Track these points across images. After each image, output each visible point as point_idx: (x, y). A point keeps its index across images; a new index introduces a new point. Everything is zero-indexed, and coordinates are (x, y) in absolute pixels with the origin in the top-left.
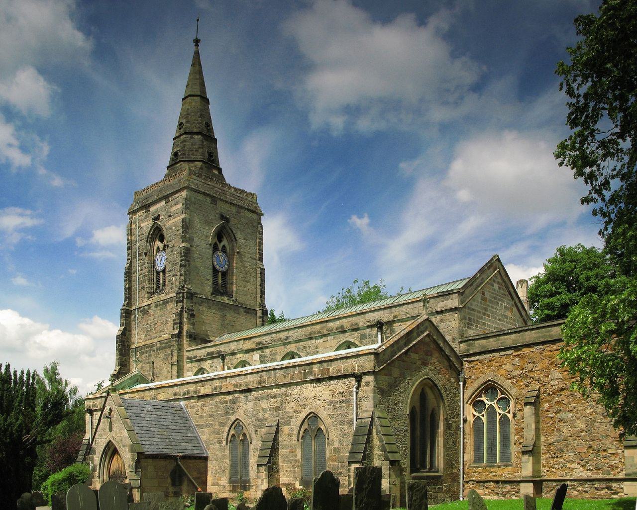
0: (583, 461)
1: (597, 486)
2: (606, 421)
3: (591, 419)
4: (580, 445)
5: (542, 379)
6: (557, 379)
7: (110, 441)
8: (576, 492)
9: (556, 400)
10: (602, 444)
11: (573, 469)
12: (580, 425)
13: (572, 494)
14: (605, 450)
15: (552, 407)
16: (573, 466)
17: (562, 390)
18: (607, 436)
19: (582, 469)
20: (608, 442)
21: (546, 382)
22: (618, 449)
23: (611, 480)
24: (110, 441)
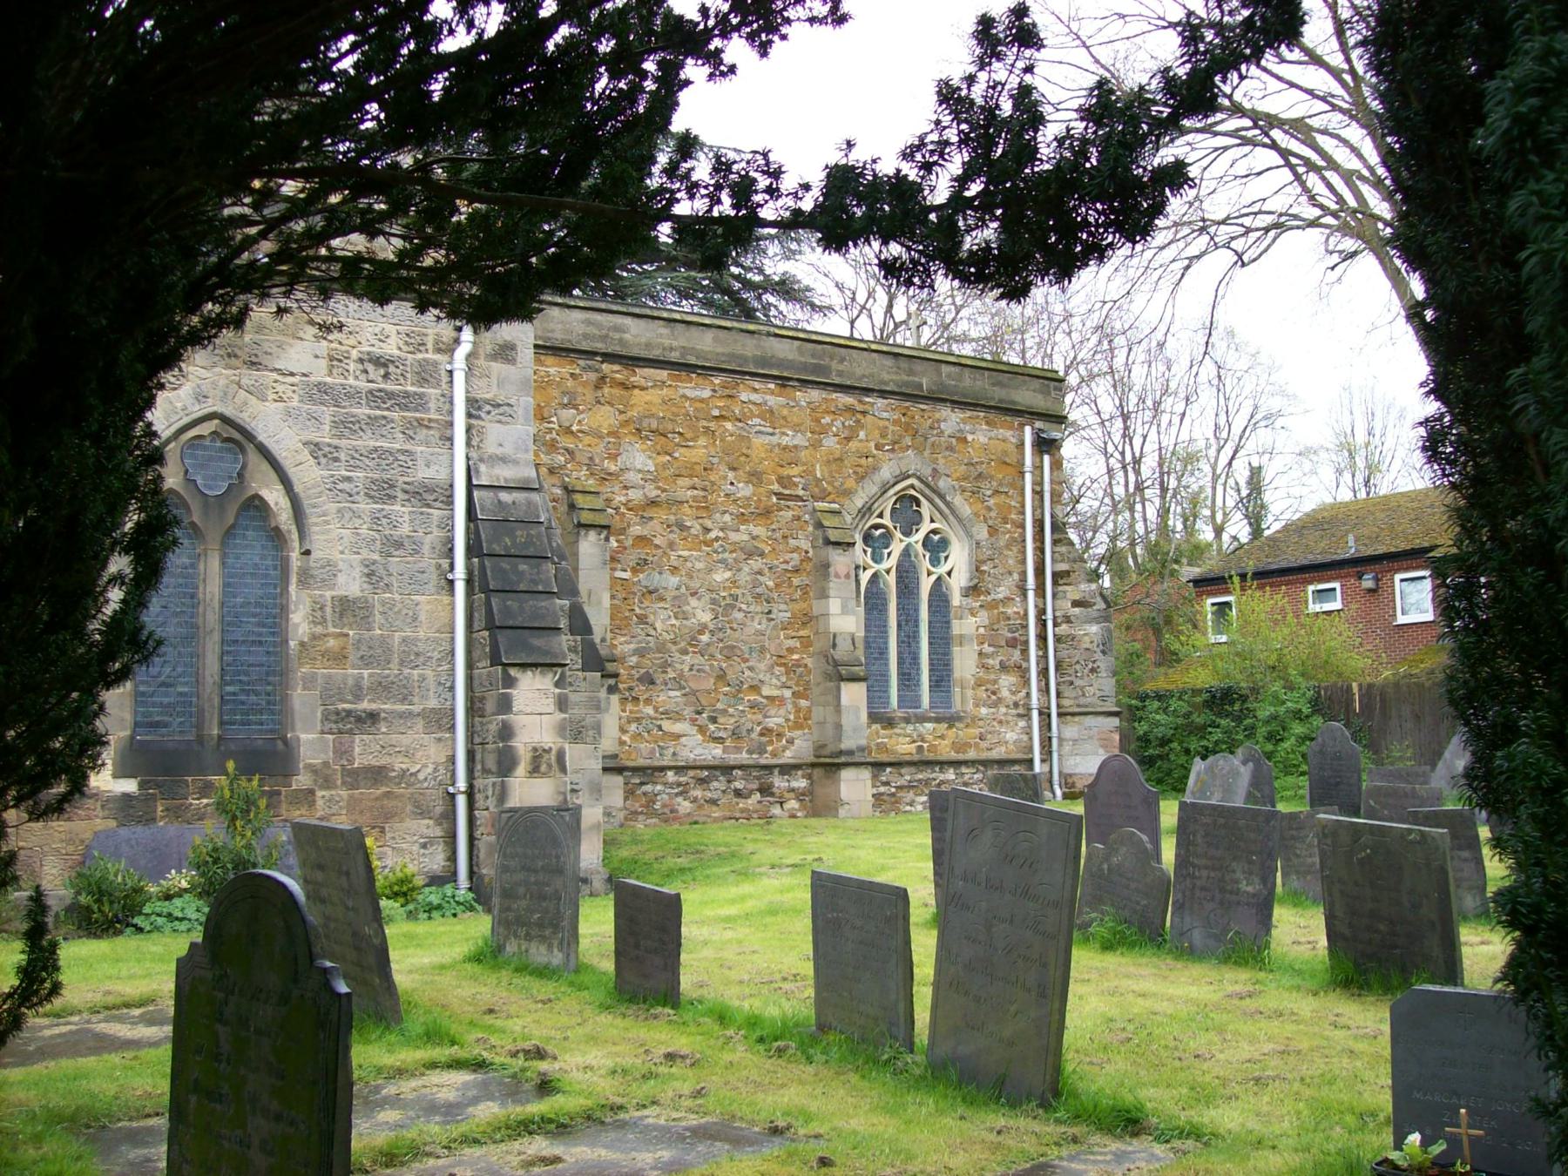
0: (704, 715)
1: (738, 785)
2: (759, 609)
3: (724, 598)
4: (698, 671)
5: (597, 461)
6: (640, 471)
7: (813, 872)
8: (687, 804)
9: (637, 530)
10: (751, 669)
11: (679, 736)
12: (699, 613)
13: (680, 808)
14: (755, 688)
15: (625, 548)
16: (678, 727)
17: (653, 503)
18: (763, 650)
19: (699, 736)
20: (762, 666)
21: (610, 474)
22: (785, 686)
23: (769, 768)
24: (813, 872)
